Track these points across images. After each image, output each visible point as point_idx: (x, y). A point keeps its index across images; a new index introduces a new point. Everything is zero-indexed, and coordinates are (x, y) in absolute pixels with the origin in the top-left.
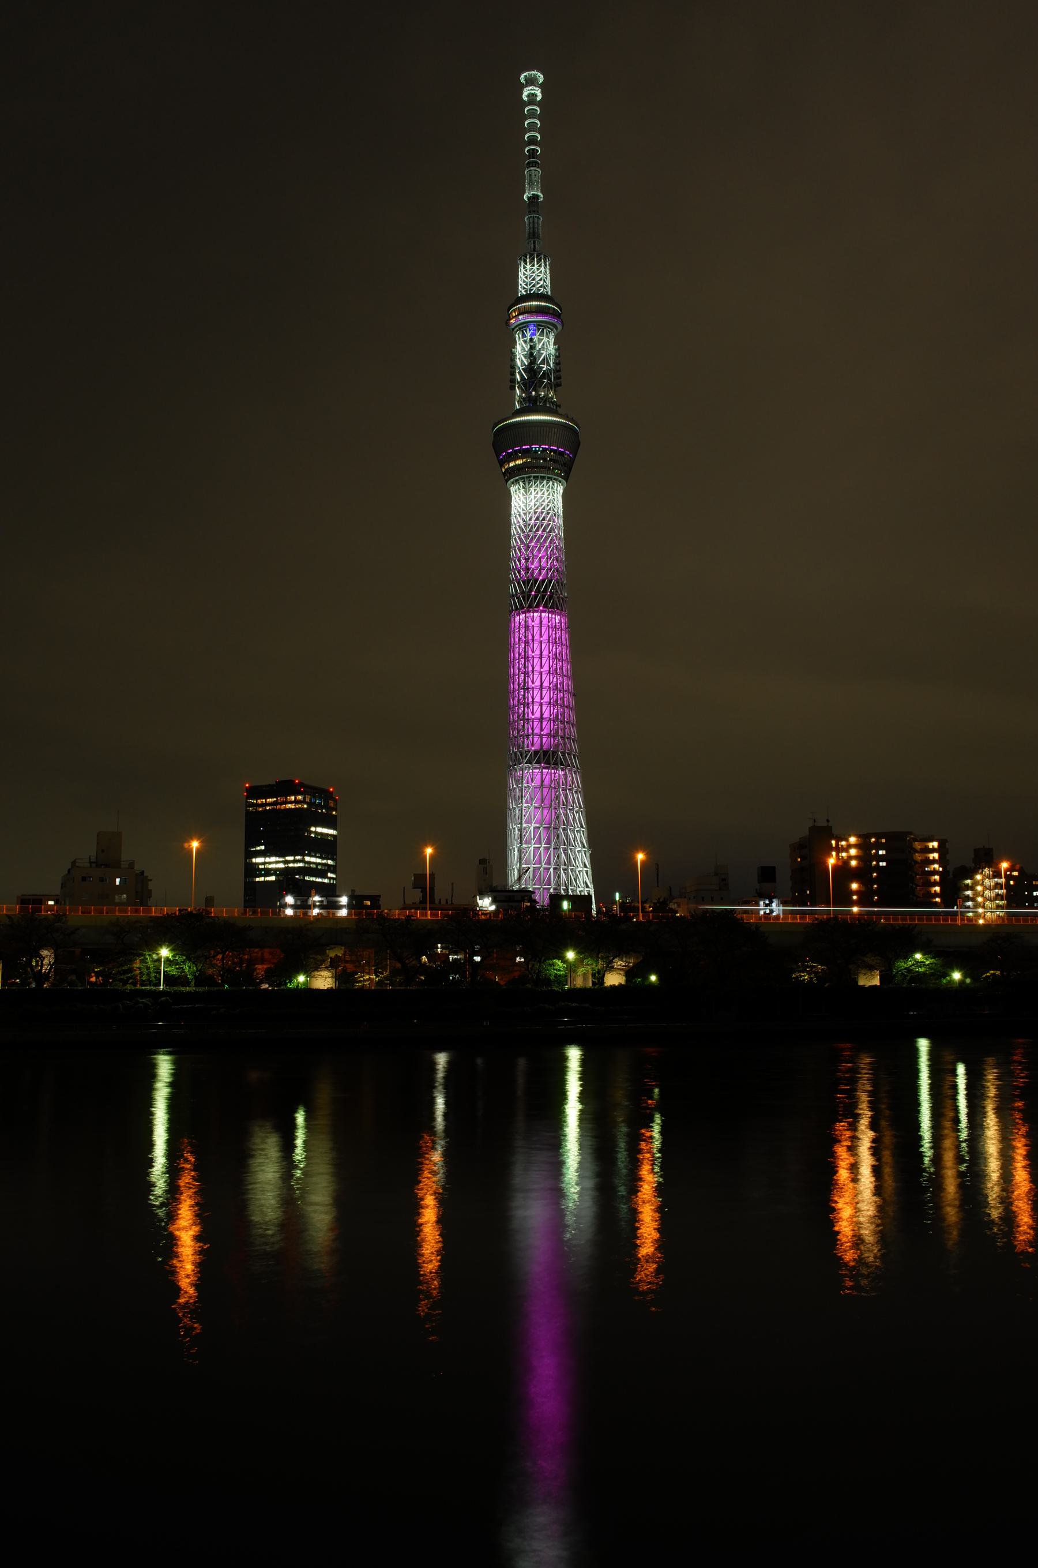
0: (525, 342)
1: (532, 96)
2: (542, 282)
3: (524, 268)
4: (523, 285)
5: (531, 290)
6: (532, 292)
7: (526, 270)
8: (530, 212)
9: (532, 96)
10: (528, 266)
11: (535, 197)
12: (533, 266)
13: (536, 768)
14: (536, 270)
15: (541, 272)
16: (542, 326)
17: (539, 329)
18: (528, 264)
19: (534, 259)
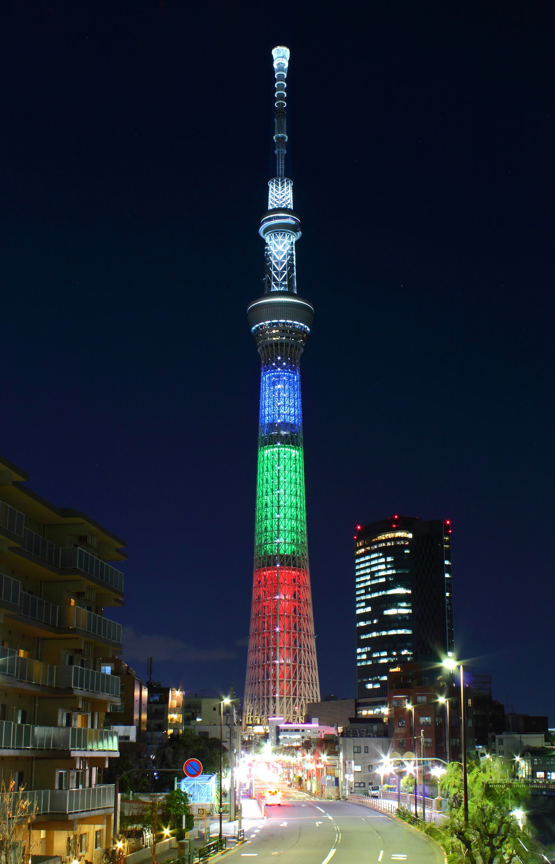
0: (277, 242)
2: (289, 201)
3: (276, 188)
4: (275, 200)
5: (282, 205)
6: (283, 207)
7: (278, 190)
8: (279, 148)
10: (280, 188)
11: (283, 138)
12: (284, 187)
13: (287, 570)
14: (285, 191)
15: (288, 193)
16: (289, 232)
17: (288, 235)
18: (280, 185)
19: (284, 183)
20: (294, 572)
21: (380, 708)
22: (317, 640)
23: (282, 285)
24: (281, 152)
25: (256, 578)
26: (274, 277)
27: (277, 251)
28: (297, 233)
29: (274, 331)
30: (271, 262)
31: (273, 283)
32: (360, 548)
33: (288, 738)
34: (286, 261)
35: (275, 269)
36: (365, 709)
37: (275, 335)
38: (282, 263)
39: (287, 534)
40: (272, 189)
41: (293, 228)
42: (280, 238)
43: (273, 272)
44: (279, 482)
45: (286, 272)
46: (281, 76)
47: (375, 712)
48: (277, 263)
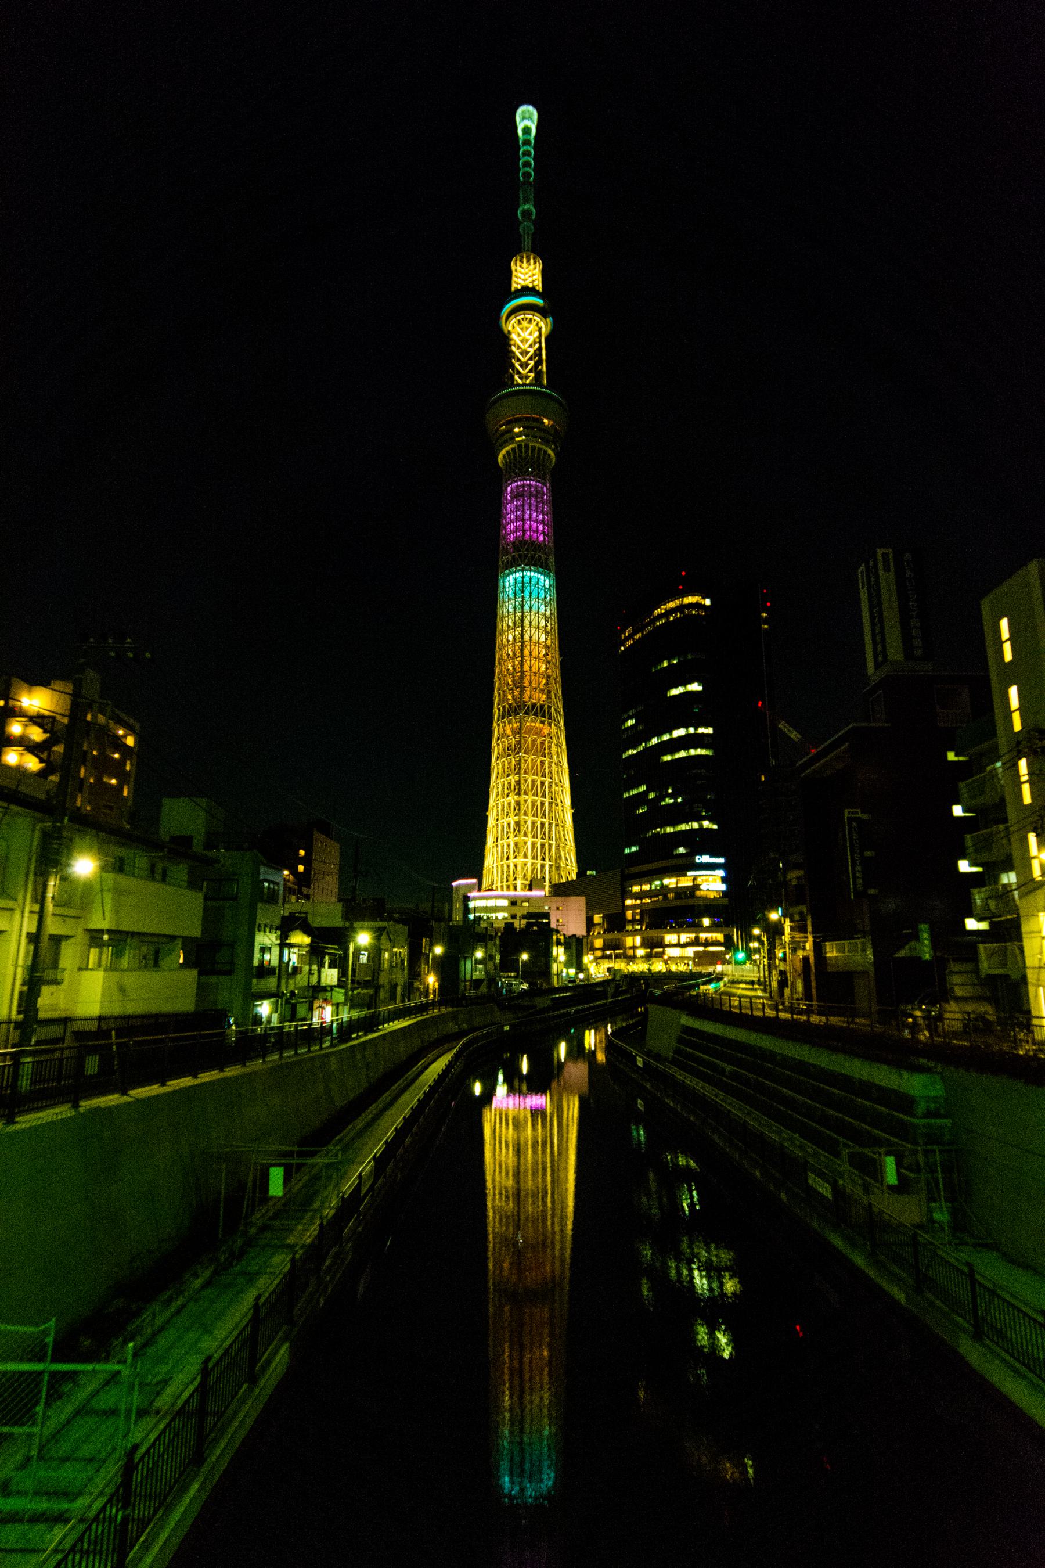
0: (522, 329)
1: (527, 130)
3: (520, 266)
4: (520, 281)
9: (527, 130)
10: (525, 265)
13: (533, 722)
20: (541, 725)
21: (661, 879)
22: (573, 814)
23: (527, 377)
24: (526, 229)
25: (496, 735)
26: (518, 370)
27: (521, 338)
28: (548, 320)
29: (516, 430)
30: (514, 353)
31: (516, 377)
32: (627, 639)
33: (485, 918)
34: (532, 351)
35: (518, 360)
36: (636, 884)
37: (519, 435)
38: (527, 353)
39: (533, 677)
40: (516, 271)
41: (543, 312)
42: (525, 324)
43: (517, 365)
44: (523, 612)
45: (532, 363)
46: (527, 153)
47: (653, 888)
48: (521, 353)
